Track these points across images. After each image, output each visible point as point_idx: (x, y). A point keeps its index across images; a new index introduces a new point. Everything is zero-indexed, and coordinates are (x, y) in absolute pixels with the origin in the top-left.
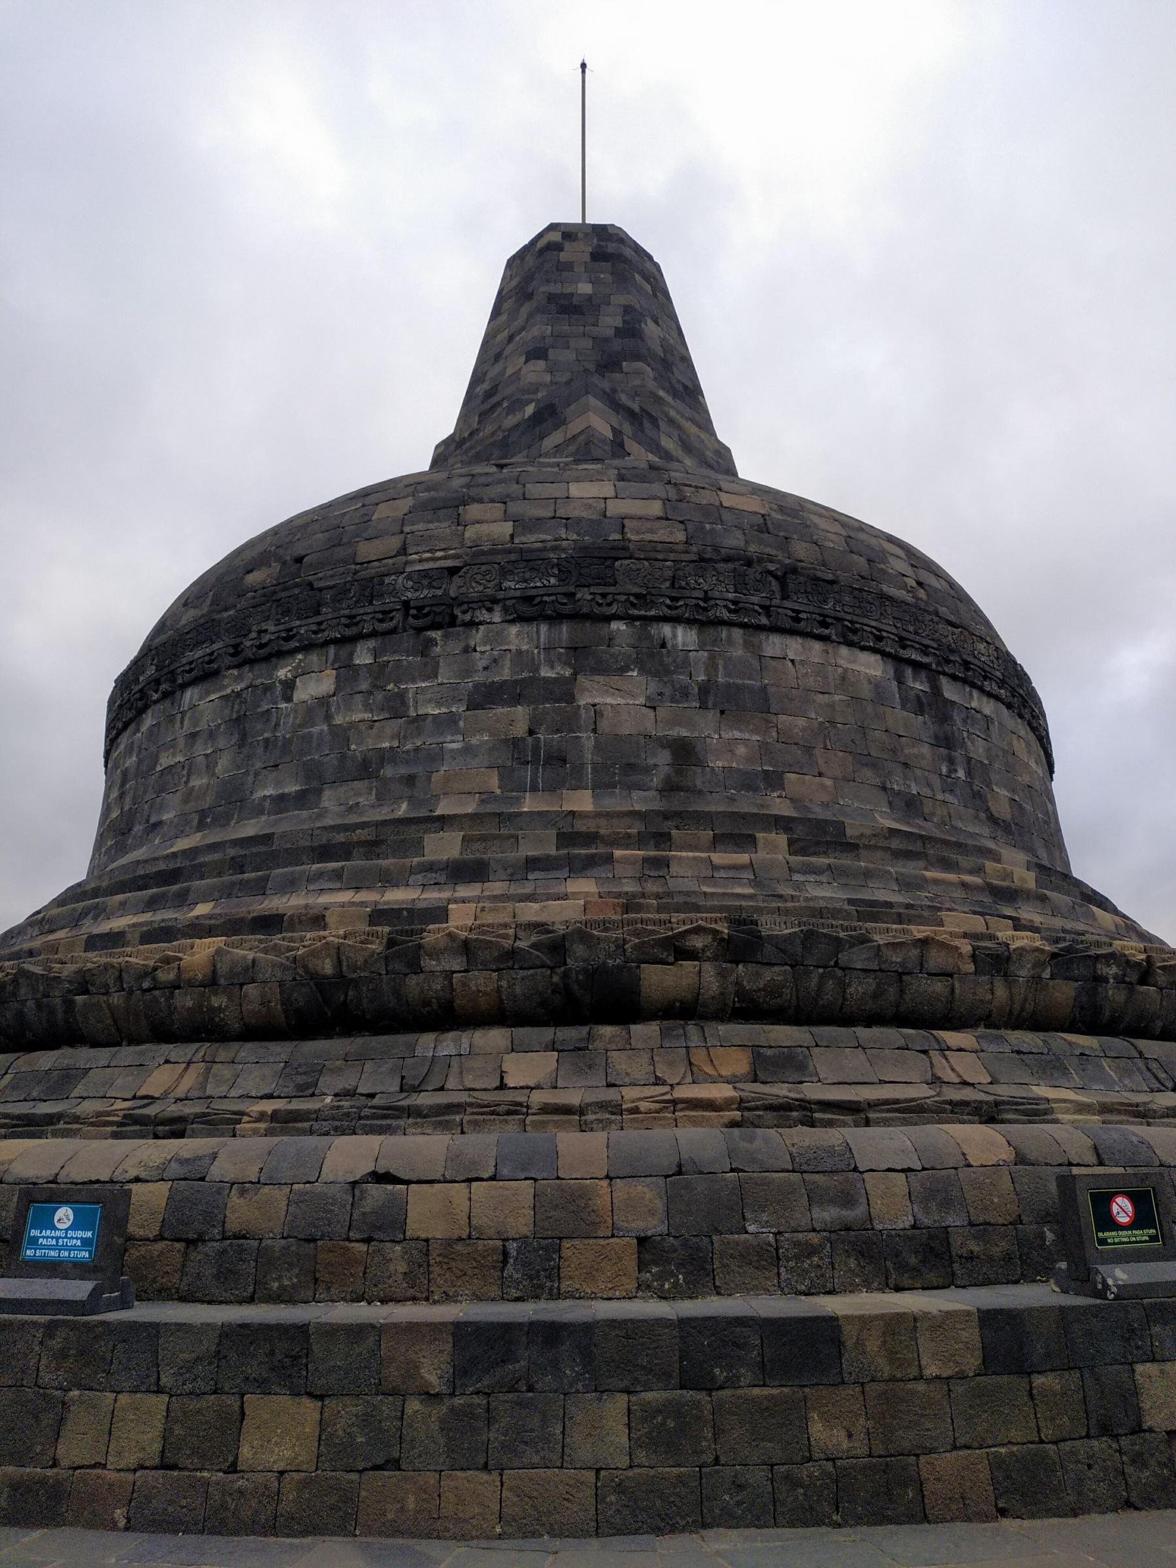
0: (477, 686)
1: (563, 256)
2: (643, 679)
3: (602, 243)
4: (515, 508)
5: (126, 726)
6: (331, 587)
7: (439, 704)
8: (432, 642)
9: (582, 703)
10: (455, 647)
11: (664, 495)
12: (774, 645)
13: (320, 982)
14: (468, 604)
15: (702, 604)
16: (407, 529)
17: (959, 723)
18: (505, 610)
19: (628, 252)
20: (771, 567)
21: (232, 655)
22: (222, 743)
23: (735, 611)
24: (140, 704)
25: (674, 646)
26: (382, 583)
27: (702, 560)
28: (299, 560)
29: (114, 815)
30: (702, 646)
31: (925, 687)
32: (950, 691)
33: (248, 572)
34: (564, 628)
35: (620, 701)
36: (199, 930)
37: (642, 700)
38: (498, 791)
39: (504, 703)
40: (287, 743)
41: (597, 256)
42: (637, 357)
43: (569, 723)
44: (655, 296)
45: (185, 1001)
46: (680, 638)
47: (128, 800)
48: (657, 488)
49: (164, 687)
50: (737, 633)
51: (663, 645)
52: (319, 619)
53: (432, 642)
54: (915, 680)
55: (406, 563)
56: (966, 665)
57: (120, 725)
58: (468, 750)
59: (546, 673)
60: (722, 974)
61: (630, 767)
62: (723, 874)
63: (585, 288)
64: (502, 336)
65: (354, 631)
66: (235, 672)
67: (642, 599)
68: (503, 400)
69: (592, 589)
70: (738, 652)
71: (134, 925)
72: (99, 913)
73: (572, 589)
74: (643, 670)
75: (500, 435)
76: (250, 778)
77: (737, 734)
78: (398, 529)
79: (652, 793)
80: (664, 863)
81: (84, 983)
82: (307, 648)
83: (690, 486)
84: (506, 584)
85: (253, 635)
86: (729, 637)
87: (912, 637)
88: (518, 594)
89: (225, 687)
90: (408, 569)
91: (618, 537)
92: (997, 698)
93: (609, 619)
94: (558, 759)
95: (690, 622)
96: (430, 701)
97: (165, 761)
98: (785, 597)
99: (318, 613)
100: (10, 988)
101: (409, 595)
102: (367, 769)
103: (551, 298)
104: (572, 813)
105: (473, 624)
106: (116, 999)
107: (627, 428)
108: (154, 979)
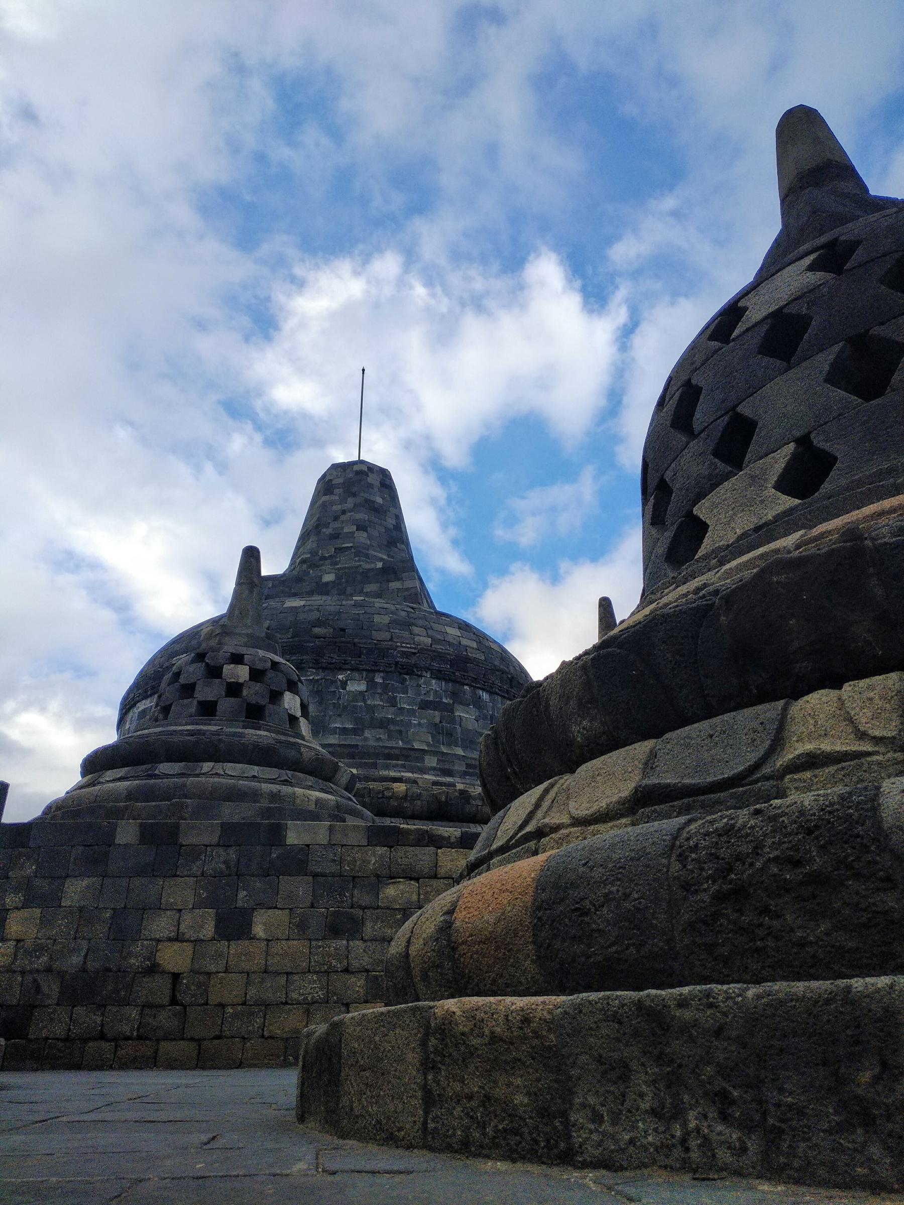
10: (414, 683)
18: (432, 674)
28: (343, 630)
38: (431, 742)
40: (345, 707)
58: (419, 724)
59: (444, 700)
65: (376, 668)
67: (475, 680)
76: (327, 718)
93: (464, 684)
94: (450, 734)
95: (487, 691)
102: (383, 724)
103: (367, 501)
105: (421, 676)
108: (383, 794)
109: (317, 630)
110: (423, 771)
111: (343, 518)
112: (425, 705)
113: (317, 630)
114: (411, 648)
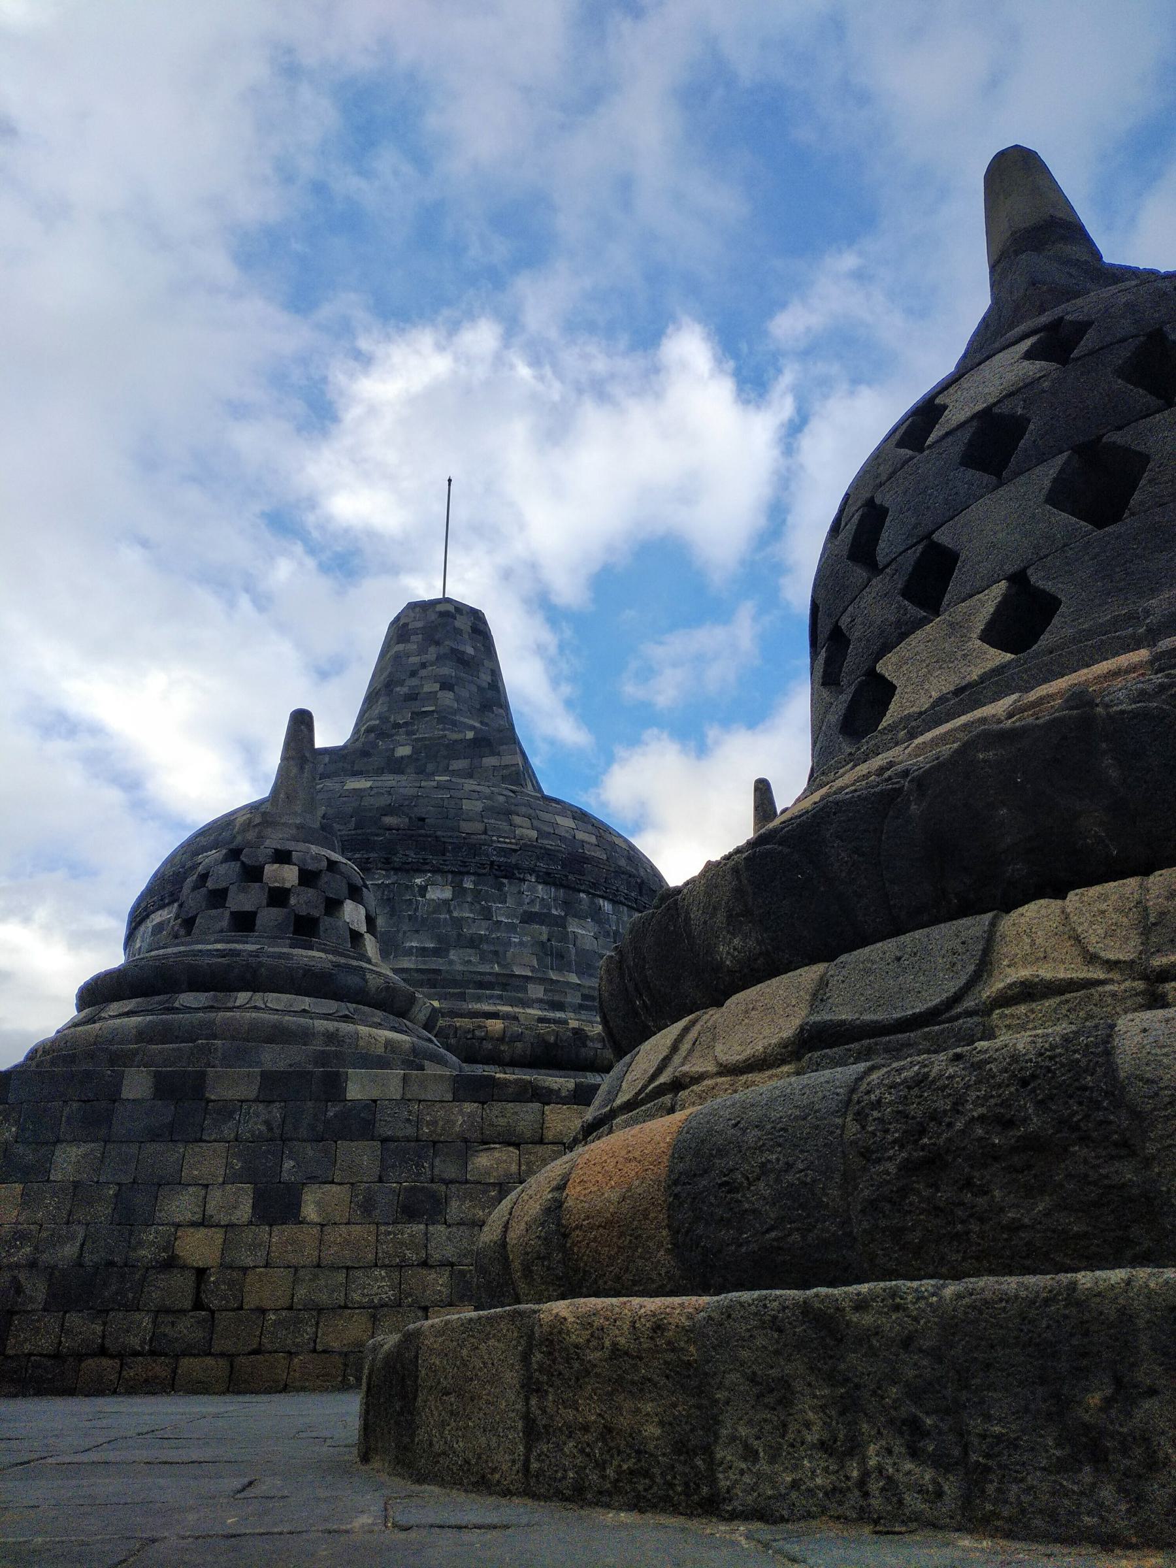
8: (503, 884)
10: (514, 890)
13: (547, 1045)
18: (538, 877)
28: (423, 820)
39: (537, 923)
40: (424, 920)
45: (488, 1045)
52: (444, 858)
53: (503, 884)
58: (521, 944)
59: (554, 912)
65: (465, 870)
67: (594, 885)
76: (400, 935)
93: (580, 891)
94: (560, 956)
95: (610, 900)
96: (503, 914)
102: (473, 943)
103: (453, 650)
105: (524, 880)
109: (388, 820)
110: (525, 1004)
111: (423, 673)
112: (529, 918)
113: (388, 820)
114: (511, 843)
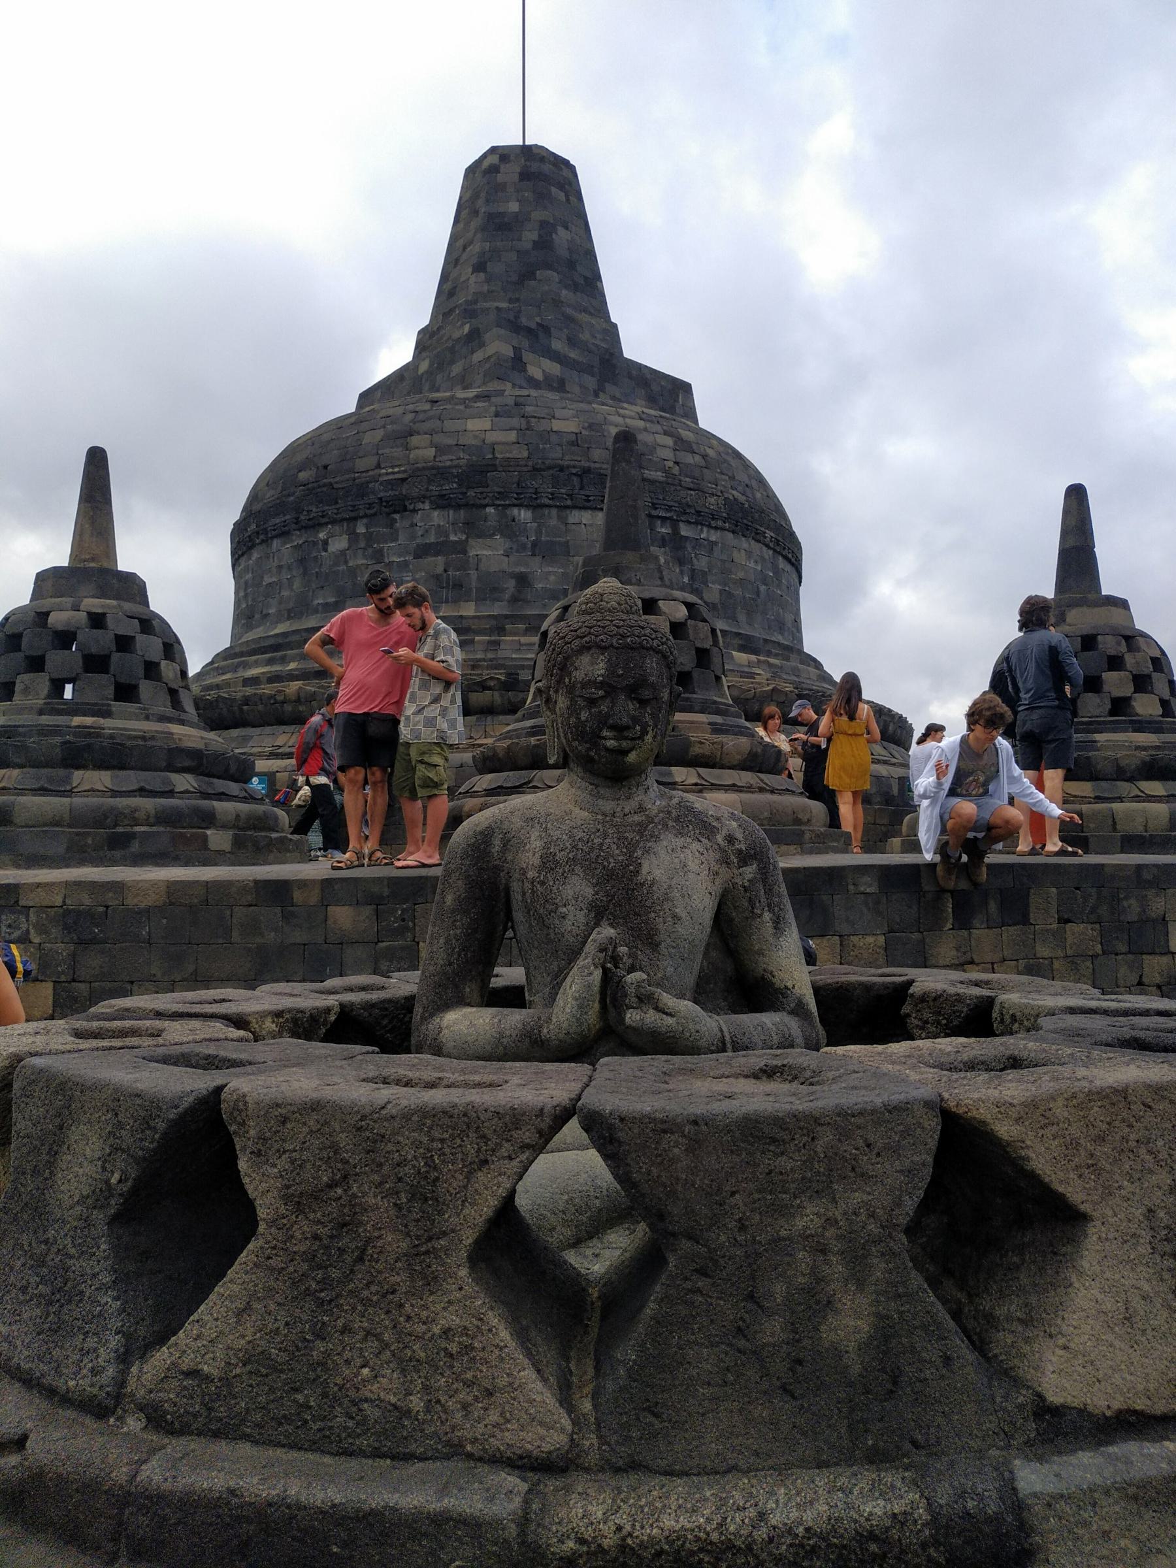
0: (418, 545)
1: (500, 178)
2: (502, 540)
3: (528, 164)
4: (439, 438)
5: (243, 555)
6: (343, 488)
7: (400, 556)
8: (395, 520)
9: (471, 554)
10: (406, 523)
11: (518, 426)
12: (574, 516)
14: (413, 500)
15: (534, 496)
16: (380, 452)
17: (689, 549)
18: (431, 502)
19: (547, 168)
20: (574, 471)
21: (296, 523)
22: (294, 573)
23: (553, 499)
24: (250, 544)
25: (519, 520)
26: (368, 487)
27: (535, 469)
28: (326, 467)
29: (244, 606)
30: (534, 520)
31: (669, 531)
32: (685, 530)
33: (300, 471)
34: (462, 512)
35: (490, 553)
36: (292, 677)
37: (502, 552)
41: (525, 176)
42: (549, 266)
43: (464, 566)
44: (568, 200)
45: (288, 708)
46: (522, 516)
47: (250, 599)
48: (515, 422)
49: (262, 537)
50: (554, 512)
51: (514, 520)
52: (338, 506)
53: (395, 520)
54: (662, 527)
55: (380, 475)
56: (698, 513)
57: (240, 553)
59: (453, 538)
60: (502, 696)
61: (495, 589)
62: (525, 648)
63: (514, 207)
64: (460, 243)
66: (298, 533)
67: (502, 495)
68: (455, 308)
69: (476, 490)
70: (553, 522)
71: (263, 673)
72: (246, 666)
73: (465, 490)
74: (502, 535)
75: (450, 344)
77: (551, 569)
78: (375, 451)
79: (505, 603)
80: (497, 643)
81: (246, 701)
82: (333, 522)
83: (535, 417)
84: (431, 488)
85: (305, 513)
86: (549, 514)
87: (660, 502)
88: (437, 493)
89: (292, 541)
90: (381, 479)
91: (490, 456)
92: (723, 529)
93: (485, 506)
94: (458, 586)
95: (528, 507)
97: (267, 580)
98: (582, 488)
99: (337, 503)
100: (214, 704)
101: (382, 494)
104: (461, 617)
105: (415, 511)
106: (260, 707)
107: (525, 343)
